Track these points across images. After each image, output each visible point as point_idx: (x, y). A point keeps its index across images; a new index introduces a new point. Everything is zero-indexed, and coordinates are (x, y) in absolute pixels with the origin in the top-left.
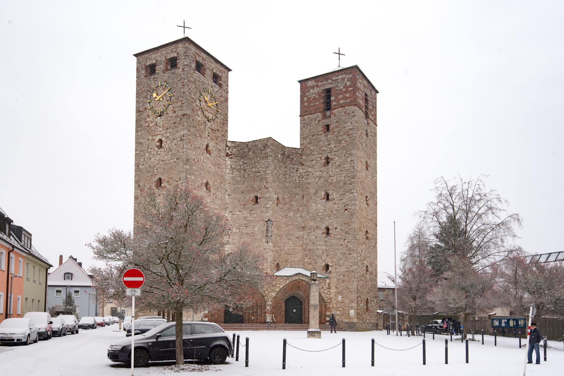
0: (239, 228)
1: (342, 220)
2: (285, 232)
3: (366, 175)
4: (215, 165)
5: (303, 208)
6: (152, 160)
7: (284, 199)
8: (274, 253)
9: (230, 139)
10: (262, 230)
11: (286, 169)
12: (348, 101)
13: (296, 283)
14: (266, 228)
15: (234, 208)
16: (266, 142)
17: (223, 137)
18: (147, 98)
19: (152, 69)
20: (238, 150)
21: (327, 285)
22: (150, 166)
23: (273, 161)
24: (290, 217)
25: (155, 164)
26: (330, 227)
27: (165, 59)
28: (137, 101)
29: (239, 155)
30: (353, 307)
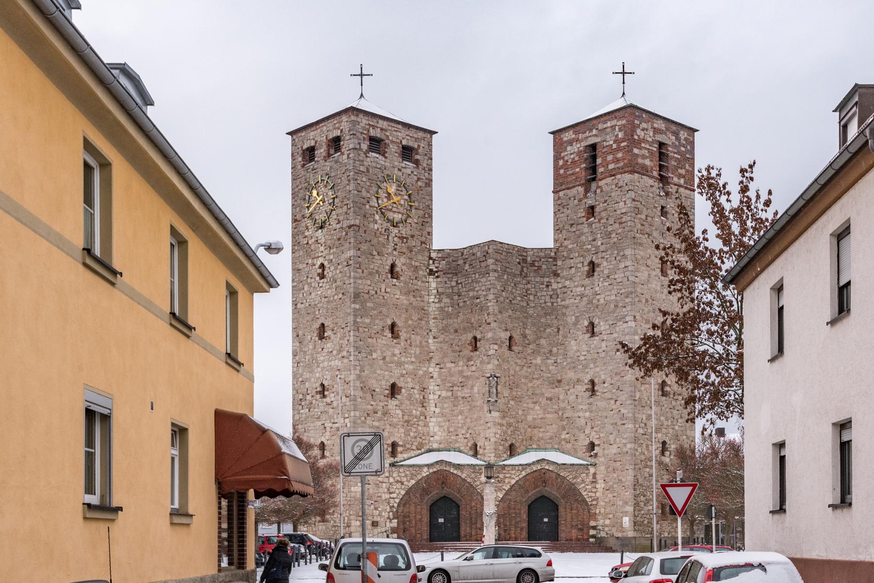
0: (451, 389)
1: (612, 367)
2: (528, 390)
3: (663, 285)
4: (407, 293)
5: (558, 349)
6: (313, 295)
7: (526, 337)
8: (504, 428)
9: (435, 246)
10: (484, 391)
11: (529, 286)
12: (621, 164)
13: (540, 475)
14: (487, 389)
15: (443, 358)
16: (487, 248)
17: (423, 245)
18: (305, 199)
19: (310, 154)
20: (448, 263)
21: (591, 477)
22: (310, 305)
23: (498, 278)
24: (536, 365)
25: (317, 302)
26: (596, 381)
27: (327, 139)
28: (293, 205)
29: (449, 272)
30: (628, 512)
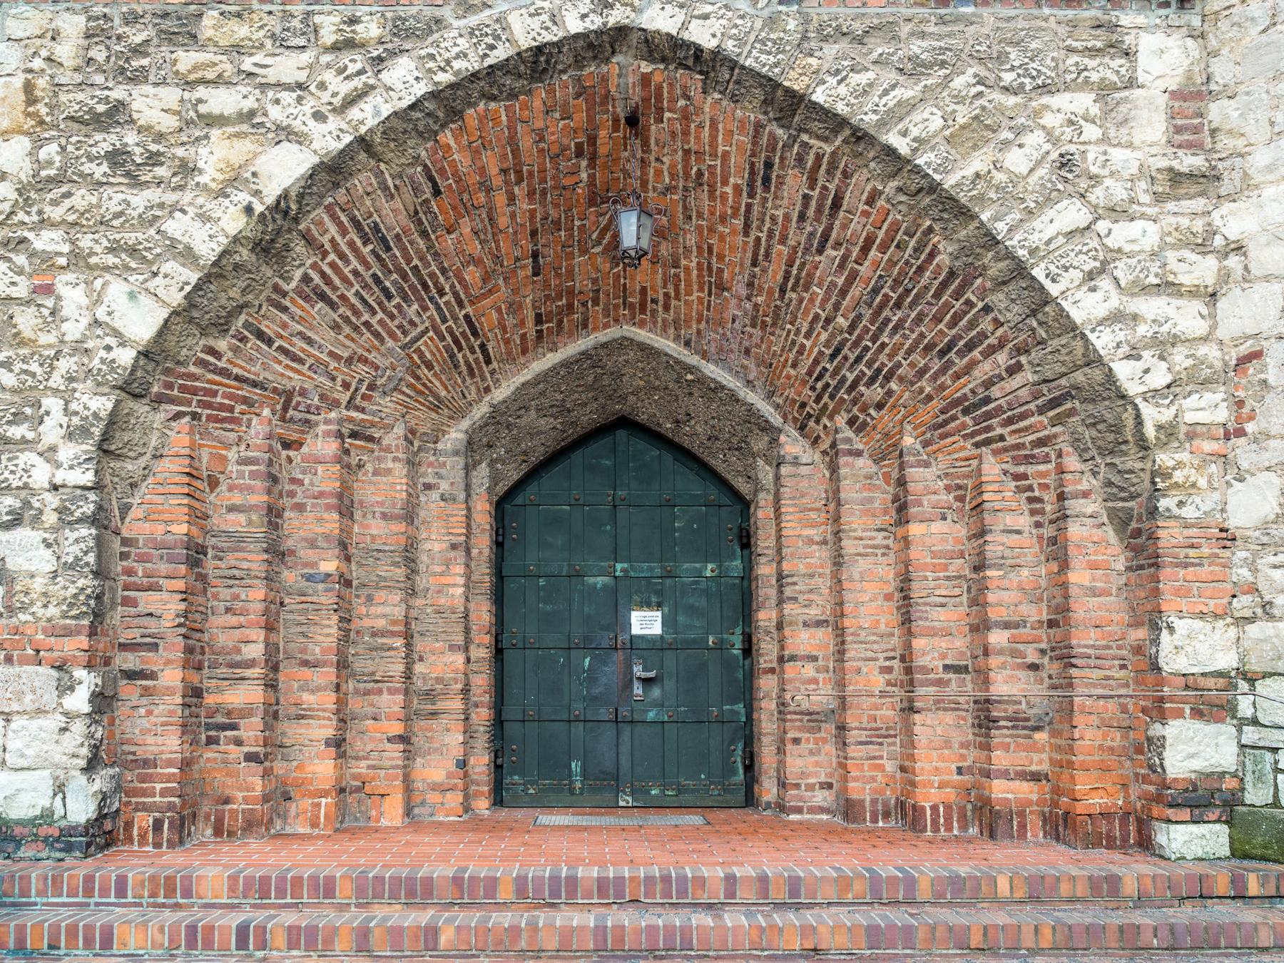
13: (587, 150)
